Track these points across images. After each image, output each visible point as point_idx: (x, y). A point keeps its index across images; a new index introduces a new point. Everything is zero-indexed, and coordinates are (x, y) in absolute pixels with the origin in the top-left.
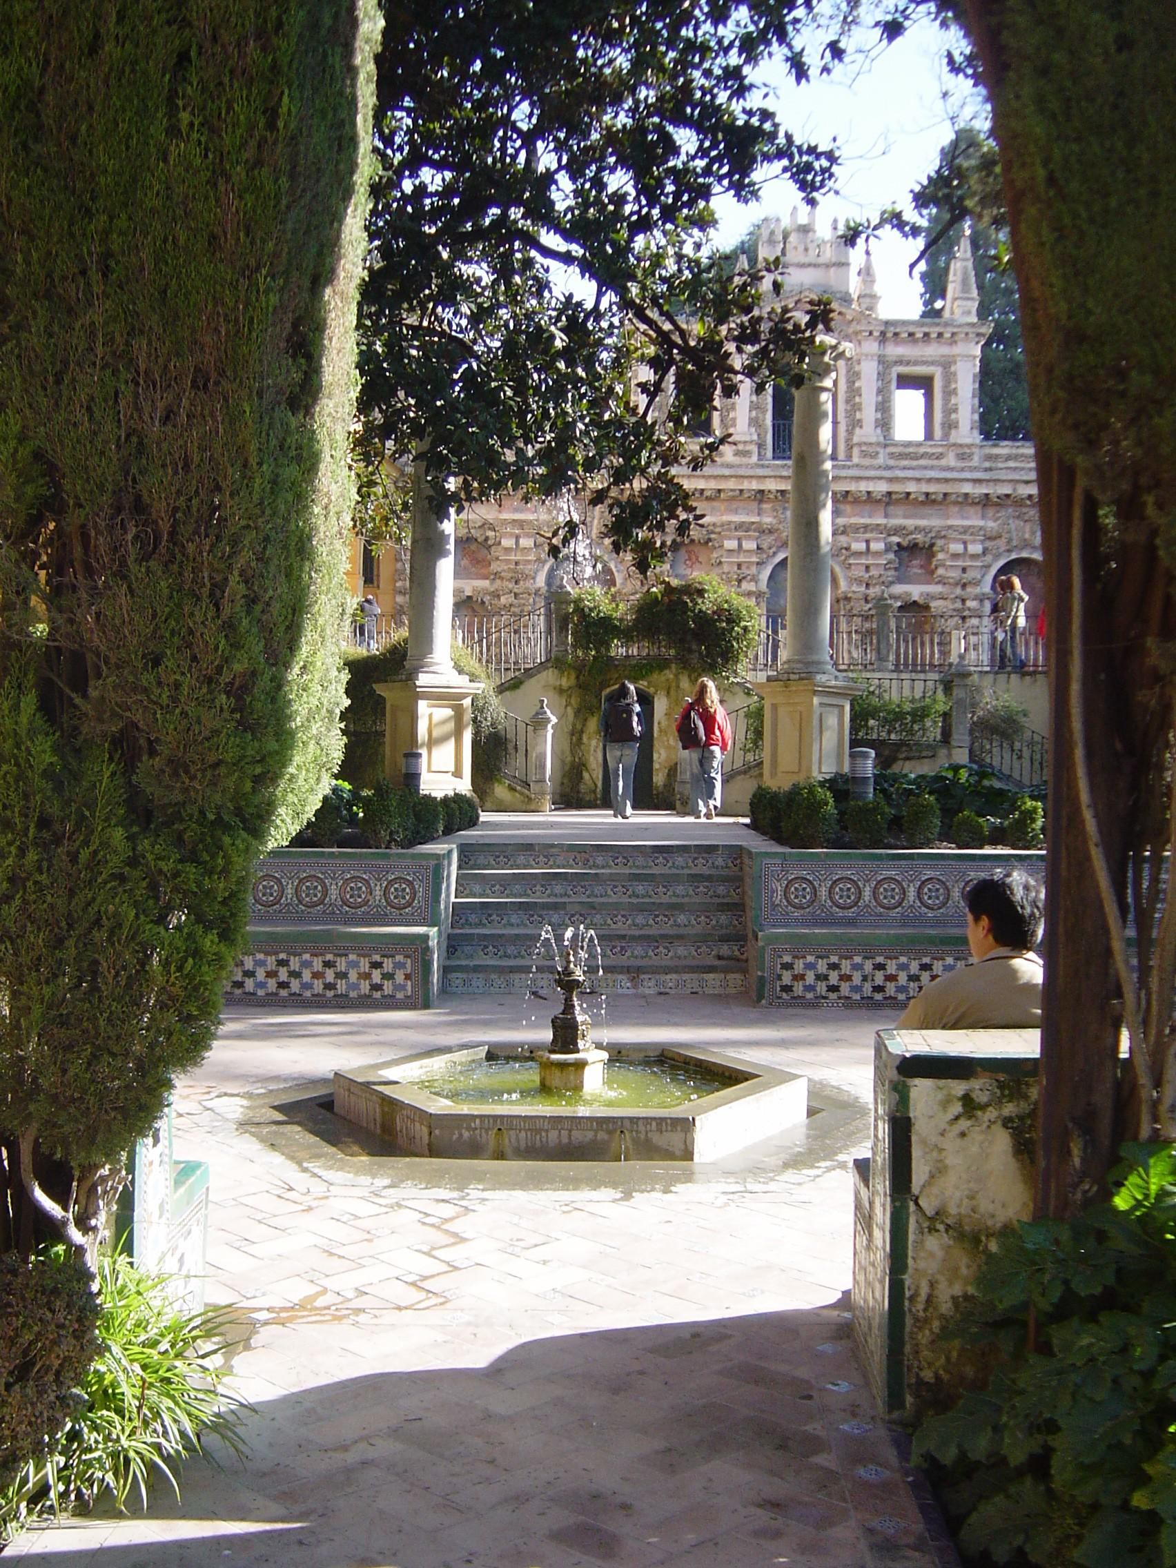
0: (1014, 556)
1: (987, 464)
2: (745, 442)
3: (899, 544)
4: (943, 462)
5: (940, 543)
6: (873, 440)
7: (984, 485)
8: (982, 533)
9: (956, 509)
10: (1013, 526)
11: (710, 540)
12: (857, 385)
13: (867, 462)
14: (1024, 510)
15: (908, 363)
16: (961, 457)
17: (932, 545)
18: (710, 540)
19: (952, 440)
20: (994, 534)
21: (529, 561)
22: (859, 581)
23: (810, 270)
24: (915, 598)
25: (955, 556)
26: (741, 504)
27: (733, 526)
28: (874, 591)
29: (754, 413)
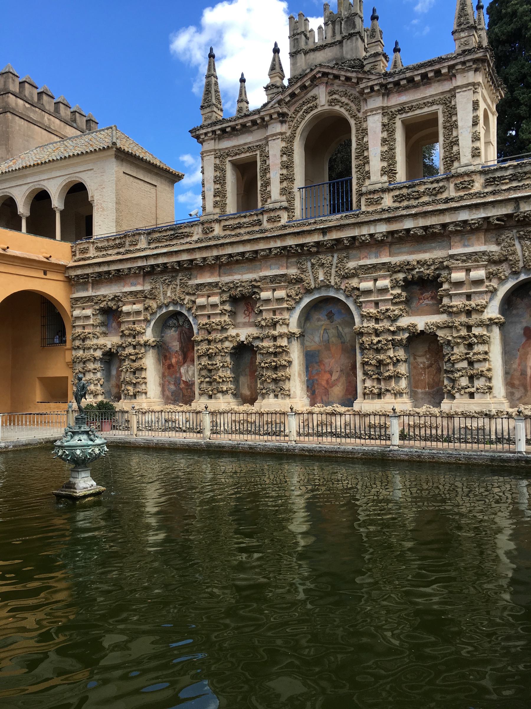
3: (405, 280)
4: (444, 196)
5: (444, 273)
6: (378, 186)
7: (482, 210)
8: (486, 257)
9: (458, 238)
11: (255, 293)
12: (365, 140)
13: (371, 209)
15: (411, 109)
16: (457, 188)
17: (439, 276)
18: (255, 293)
19: (453, 172)
20: (496, 258)
21: (140, 321)
22: (369, 317)
23: (327, 50)
24: (421, 327)
25: (459, 284)
26: (273, 261)
27: (269, 281)
28: (386, 324)
29: (285, 184)
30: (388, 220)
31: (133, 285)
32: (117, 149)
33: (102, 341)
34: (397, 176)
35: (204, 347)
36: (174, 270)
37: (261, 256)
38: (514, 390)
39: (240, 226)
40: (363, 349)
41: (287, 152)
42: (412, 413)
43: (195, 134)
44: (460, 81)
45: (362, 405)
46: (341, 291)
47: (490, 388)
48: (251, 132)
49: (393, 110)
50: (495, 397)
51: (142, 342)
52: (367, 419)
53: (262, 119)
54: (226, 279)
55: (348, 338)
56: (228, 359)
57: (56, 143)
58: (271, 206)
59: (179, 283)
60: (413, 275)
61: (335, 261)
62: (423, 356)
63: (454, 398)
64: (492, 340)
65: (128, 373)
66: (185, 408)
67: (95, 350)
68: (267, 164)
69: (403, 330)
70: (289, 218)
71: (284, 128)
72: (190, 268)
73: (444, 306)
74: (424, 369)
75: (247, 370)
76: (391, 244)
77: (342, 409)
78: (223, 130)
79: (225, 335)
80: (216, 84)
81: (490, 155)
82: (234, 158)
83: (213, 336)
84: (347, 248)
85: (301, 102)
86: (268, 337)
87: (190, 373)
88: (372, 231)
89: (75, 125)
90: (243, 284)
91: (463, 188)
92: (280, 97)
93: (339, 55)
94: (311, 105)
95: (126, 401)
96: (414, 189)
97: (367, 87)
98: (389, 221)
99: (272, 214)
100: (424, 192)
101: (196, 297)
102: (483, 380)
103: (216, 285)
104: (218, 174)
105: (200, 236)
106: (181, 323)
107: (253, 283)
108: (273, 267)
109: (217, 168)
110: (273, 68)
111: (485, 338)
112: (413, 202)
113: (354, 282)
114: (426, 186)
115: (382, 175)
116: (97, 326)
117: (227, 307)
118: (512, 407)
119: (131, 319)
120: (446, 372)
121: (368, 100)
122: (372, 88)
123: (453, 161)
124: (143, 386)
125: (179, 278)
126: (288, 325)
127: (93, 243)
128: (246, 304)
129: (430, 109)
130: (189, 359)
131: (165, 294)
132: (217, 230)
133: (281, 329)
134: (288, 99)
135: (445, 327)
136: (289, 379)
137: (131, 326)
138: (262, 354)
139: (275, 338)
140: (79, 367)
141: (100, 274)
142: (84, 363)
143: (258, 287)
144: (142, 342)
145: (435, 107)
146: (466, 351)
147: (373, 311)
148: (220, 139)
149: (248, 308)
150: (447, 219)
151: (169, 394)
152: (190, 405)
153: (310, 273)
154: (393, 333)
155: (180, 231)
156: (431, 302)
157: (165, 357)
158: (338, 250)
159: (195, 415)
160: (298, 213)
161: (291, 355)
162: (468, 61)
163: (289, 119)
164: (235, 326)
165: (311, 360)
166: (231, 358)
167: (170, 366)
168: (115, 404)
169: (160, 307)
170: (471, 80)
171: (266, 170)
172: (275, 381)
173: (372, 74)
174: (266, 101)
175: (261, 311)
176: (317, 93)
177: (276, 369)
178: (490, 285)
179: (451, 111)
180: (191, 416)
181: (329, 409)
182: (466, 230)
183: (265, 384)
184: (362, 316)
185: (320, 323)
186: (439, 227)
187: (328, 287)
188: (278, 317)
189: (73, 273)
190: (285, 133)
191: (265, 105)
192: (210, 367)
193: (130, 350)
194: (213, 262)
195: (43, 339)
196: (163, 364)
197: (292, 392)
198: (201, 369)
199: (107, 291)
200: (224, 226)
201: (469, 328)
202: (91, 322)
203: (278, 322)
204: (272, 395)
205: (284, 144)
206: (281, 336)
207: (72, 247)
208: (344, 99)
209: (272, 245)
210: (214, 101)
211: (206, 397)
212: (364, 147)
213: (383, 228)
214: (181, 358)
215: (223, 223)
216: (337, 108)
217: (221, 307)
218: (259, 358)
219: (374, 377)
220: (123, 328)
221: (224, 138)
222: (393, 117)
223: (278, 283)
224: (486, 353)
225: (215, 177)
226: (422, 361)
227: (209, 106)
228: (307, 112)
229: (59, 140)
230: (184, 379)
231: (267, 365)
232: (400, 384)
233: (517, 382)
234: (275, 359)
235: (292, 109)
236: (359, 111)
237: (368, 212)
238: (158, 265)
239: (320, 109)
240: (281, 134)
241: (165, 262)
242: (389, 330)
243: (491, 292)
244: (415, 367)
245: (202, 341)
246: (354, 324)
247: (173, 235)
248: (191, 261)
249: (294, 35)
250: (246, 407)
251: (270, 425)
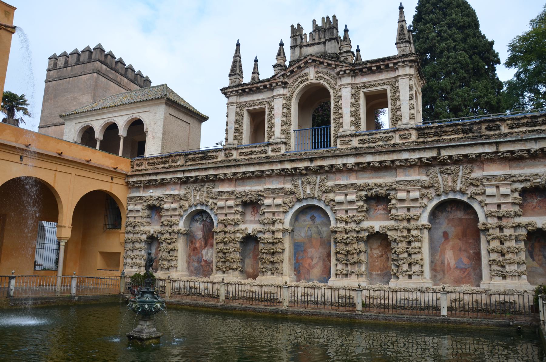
0: (443, 198)
1: (421, 140)
2: (277, 143)
3: (366, 196)
5: (392, 193)
8: (420, 184)
10: (440, 178)
11: (260, 200)
12: (340, 103)
13: (344, 147)
14: (448, 167)
15: (370, 86)
16: (401, 137)
17: (389, 194)
18: (260, 200)
19: (398, 127)
20: (426, 185)
22: (341, 220)
24: (377, 229)
25: (402, 200)
26: (275, 178)
27: (270, 192)
28: (353, 225)
29: (284, 127)
30: (356, 155)
31: (172, 190)
32: (167, 98)
33: (147, 228)
34: (361, 127)
35: (221, 236)
36: (202, 181)
37: (266, 175)
38: (436, 274)
39: (251, 153)
40: (336, 243)
41: (287, 107)
42: (369, 288)
43: (225, 91)
44: (401, 72)
45: (334, 281)
46: (322, 202)
47: (422, 272)
48: (262, 92)
49: (358, 86)
50: (425, 278)
51: (176, 231)
52: (337, 292)
53: (271, 85)
55: (325, 234)
56: (238, 245)
57: (125, 93)
58: (274, 141)
59: (205, 190)
60: (372, 193)
61: (318, 180)
62: (377, 249)
63: (398, 278)
64: (423, 239)
65: (165, 252)
66: (205, 279)
67: (142, 234)
68: (273, 113)
69: (364, 230)
70: (286, 150)
71: (285, 91)
72: (216, 180)
73: (392, 215)
74: (377, 258)
75: (251, 254)
76: (357, 171)
77: (320, 285)
78: (244, 90)
79: (237, 228)
80: (240, 61)
81: (419, 120)
82: (250, 108)
83: (229, 228)
84: (327, 172)
85: (297, 76)
86: (268, 231)
87: (209, 254)
88: (345, 162)
89: (136, 83)
90: (252, 193)
91: (404, 138)
92: (283, 72)
93: (323, 50)
95: (161, 272)
96: (372, 136)
97: (341, 71)
98: (356, 156)
99: (275, 147)
100: (379, 139)
101: (217, 200)
102: (417, 266)
103: (233, 192)
104: (238, 118)
105: (223, 158)
106: (204, 219)
107: (259, 193)
108: (274, 182)
109: (237, 114)
110: (279, 54)
111: (419, 238)
112: (372, 145)
113: (331, 196)
114: (380, 135)
115: (351, 126)
116: (144, 218)
117: (240, 209)
118: (435, 285)
119: (169, 213)
120: (393, 260)
121: (342, 79)
122: (345, 71)
123: (397, 121)
124: (175, 263)
125: (206, 187)
126: (283, 223)
127: (146, 160)
128: (253, 207)
129: (382, 87)
130: (209, 245)
131: (195, 197)
132: (235, 155)
133: (278, 226)
134: (289, 74)
135: (393, 230)
136: (282, 262)
137: (169, 218)
138: (264, 243)
139: (273, 232)
140: (129, 246)
141: (149, 181)
142: (133, 243)
143: (263, 196)
144: (176, 231)
145: (385, 87)
146: (407, 246)
147: (344, 216)
148: (240, 96)
149: (254, 210)
150: (395, 157)
151: (193, 269)
152: (209, 278)
153: (301, 188)
154: (358, 232)
155: (209, 154)
156: (383, 212)
157: (192, 242)
158: (320, 173)
159: (211, 284)
160: (293, 147)
161: (285, 245)
162: (406, 61)
163: (289, 86)
164: (244, 222)
165: (299, 249)
166: (240, 245)
167: (195, 249)
168: (155, 274)
169: (190, 207)
170: (408, 72)
171: (272, 117)
172: (272, 263)
173: (345, 63)
174: (273, 74)
175: (264, 213)
176: (308, 72)
177: (273, 254)
178: (422, 203)
179: (396, 90)
180: (208, 285)
181: (311, 284)
182: (407, 165)
183: (265, 264)
184: (337, 220)
185: (306, 223)
186: (389, 162)
187: (313, 198)
188: (276, 217)
189: (131, 180)
190: (286, 95)
191: (273, 77)
192: (226, 251)
193: (167, 236)
194: (231, 177)
195: (105, 225)
196: (190, 247)
197: (284, 271)
198: (218, 252)
199: (154, 193)
200: (241, 153)
201: (409, 230)
202: (140, 214)
203: (276, 221)
204: (269, 273)
205: (285, 102)
206: (278, 231)
207: (131, 162)
208: (326, 77)
209: (275, 167)
210: (238, 72)
211: (221, 272)
212: (339, 107)
213: (351, 161)
214: (203, 243)
215: (240, 151)
216: (321, 82)
217: (235, 209)
218: (261, 246)
219: (343, 262)
220: (163, 219)
221: (243, 95)
222: (358, 90)
224: (420, 248)
225: (236, 120)
226: (377, 252)
227: (235, 75)
229: (126, 92)
230: (204, 258)
231: (266, 251)
232: (361, 268)
233: (438, 268)
234: (273, 247)
235: (291, 80)
237: (342, 149)
238: (191, 177)
239: (310, 81)
240: (283, 95)
241: (197, 175)
242: (355, 230)
243: (423, 207)
244: (371, 257)
245: (220, 232)
246: (330, 224)
247: (204, 157)
248: (216, 175)
249: (294, 36)
250: (250, 281)
251: (266, 295)
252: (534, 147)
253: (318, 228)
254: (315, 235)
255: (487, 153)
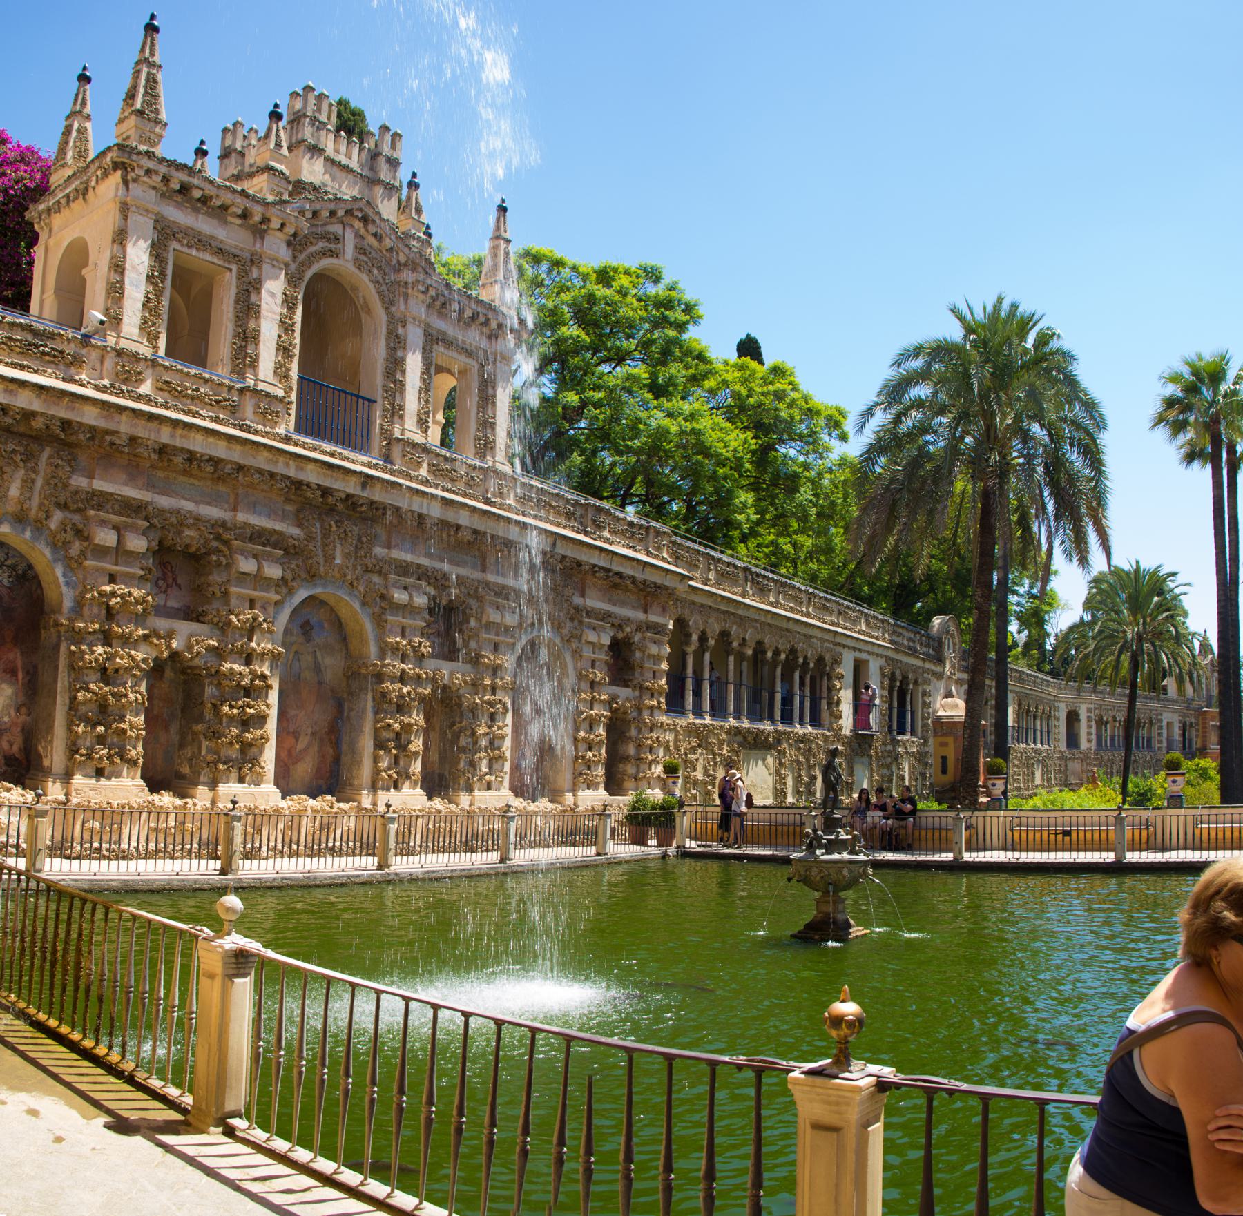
5: (473, 603)
54: (164, 502)
58: (261, 386)
94: (333, 246)
143: (226, 543)
149: (164, 574)
204: (234, 775)
211: (92, 771)
218: (210, 691)
223: (264, 545)
228: (324, 253)
231: (235, 711)
236: (392, 303)
252: (640, 576)
253: (315, 657)
254: (308, 675)
255: (601, 568)
